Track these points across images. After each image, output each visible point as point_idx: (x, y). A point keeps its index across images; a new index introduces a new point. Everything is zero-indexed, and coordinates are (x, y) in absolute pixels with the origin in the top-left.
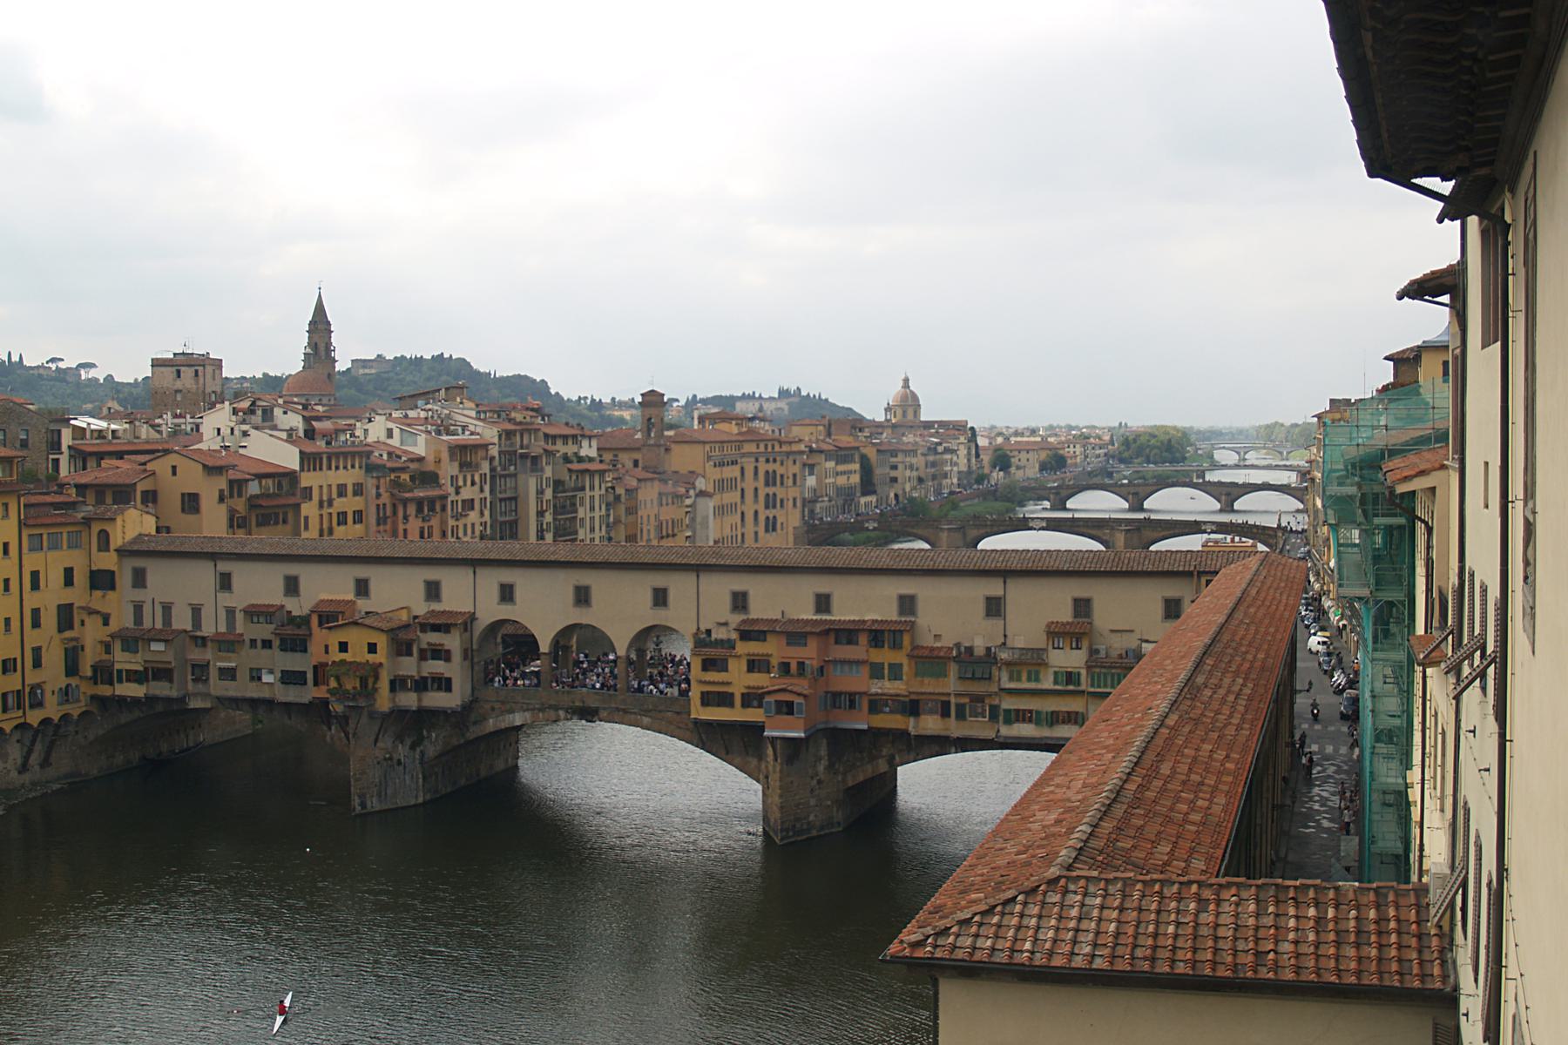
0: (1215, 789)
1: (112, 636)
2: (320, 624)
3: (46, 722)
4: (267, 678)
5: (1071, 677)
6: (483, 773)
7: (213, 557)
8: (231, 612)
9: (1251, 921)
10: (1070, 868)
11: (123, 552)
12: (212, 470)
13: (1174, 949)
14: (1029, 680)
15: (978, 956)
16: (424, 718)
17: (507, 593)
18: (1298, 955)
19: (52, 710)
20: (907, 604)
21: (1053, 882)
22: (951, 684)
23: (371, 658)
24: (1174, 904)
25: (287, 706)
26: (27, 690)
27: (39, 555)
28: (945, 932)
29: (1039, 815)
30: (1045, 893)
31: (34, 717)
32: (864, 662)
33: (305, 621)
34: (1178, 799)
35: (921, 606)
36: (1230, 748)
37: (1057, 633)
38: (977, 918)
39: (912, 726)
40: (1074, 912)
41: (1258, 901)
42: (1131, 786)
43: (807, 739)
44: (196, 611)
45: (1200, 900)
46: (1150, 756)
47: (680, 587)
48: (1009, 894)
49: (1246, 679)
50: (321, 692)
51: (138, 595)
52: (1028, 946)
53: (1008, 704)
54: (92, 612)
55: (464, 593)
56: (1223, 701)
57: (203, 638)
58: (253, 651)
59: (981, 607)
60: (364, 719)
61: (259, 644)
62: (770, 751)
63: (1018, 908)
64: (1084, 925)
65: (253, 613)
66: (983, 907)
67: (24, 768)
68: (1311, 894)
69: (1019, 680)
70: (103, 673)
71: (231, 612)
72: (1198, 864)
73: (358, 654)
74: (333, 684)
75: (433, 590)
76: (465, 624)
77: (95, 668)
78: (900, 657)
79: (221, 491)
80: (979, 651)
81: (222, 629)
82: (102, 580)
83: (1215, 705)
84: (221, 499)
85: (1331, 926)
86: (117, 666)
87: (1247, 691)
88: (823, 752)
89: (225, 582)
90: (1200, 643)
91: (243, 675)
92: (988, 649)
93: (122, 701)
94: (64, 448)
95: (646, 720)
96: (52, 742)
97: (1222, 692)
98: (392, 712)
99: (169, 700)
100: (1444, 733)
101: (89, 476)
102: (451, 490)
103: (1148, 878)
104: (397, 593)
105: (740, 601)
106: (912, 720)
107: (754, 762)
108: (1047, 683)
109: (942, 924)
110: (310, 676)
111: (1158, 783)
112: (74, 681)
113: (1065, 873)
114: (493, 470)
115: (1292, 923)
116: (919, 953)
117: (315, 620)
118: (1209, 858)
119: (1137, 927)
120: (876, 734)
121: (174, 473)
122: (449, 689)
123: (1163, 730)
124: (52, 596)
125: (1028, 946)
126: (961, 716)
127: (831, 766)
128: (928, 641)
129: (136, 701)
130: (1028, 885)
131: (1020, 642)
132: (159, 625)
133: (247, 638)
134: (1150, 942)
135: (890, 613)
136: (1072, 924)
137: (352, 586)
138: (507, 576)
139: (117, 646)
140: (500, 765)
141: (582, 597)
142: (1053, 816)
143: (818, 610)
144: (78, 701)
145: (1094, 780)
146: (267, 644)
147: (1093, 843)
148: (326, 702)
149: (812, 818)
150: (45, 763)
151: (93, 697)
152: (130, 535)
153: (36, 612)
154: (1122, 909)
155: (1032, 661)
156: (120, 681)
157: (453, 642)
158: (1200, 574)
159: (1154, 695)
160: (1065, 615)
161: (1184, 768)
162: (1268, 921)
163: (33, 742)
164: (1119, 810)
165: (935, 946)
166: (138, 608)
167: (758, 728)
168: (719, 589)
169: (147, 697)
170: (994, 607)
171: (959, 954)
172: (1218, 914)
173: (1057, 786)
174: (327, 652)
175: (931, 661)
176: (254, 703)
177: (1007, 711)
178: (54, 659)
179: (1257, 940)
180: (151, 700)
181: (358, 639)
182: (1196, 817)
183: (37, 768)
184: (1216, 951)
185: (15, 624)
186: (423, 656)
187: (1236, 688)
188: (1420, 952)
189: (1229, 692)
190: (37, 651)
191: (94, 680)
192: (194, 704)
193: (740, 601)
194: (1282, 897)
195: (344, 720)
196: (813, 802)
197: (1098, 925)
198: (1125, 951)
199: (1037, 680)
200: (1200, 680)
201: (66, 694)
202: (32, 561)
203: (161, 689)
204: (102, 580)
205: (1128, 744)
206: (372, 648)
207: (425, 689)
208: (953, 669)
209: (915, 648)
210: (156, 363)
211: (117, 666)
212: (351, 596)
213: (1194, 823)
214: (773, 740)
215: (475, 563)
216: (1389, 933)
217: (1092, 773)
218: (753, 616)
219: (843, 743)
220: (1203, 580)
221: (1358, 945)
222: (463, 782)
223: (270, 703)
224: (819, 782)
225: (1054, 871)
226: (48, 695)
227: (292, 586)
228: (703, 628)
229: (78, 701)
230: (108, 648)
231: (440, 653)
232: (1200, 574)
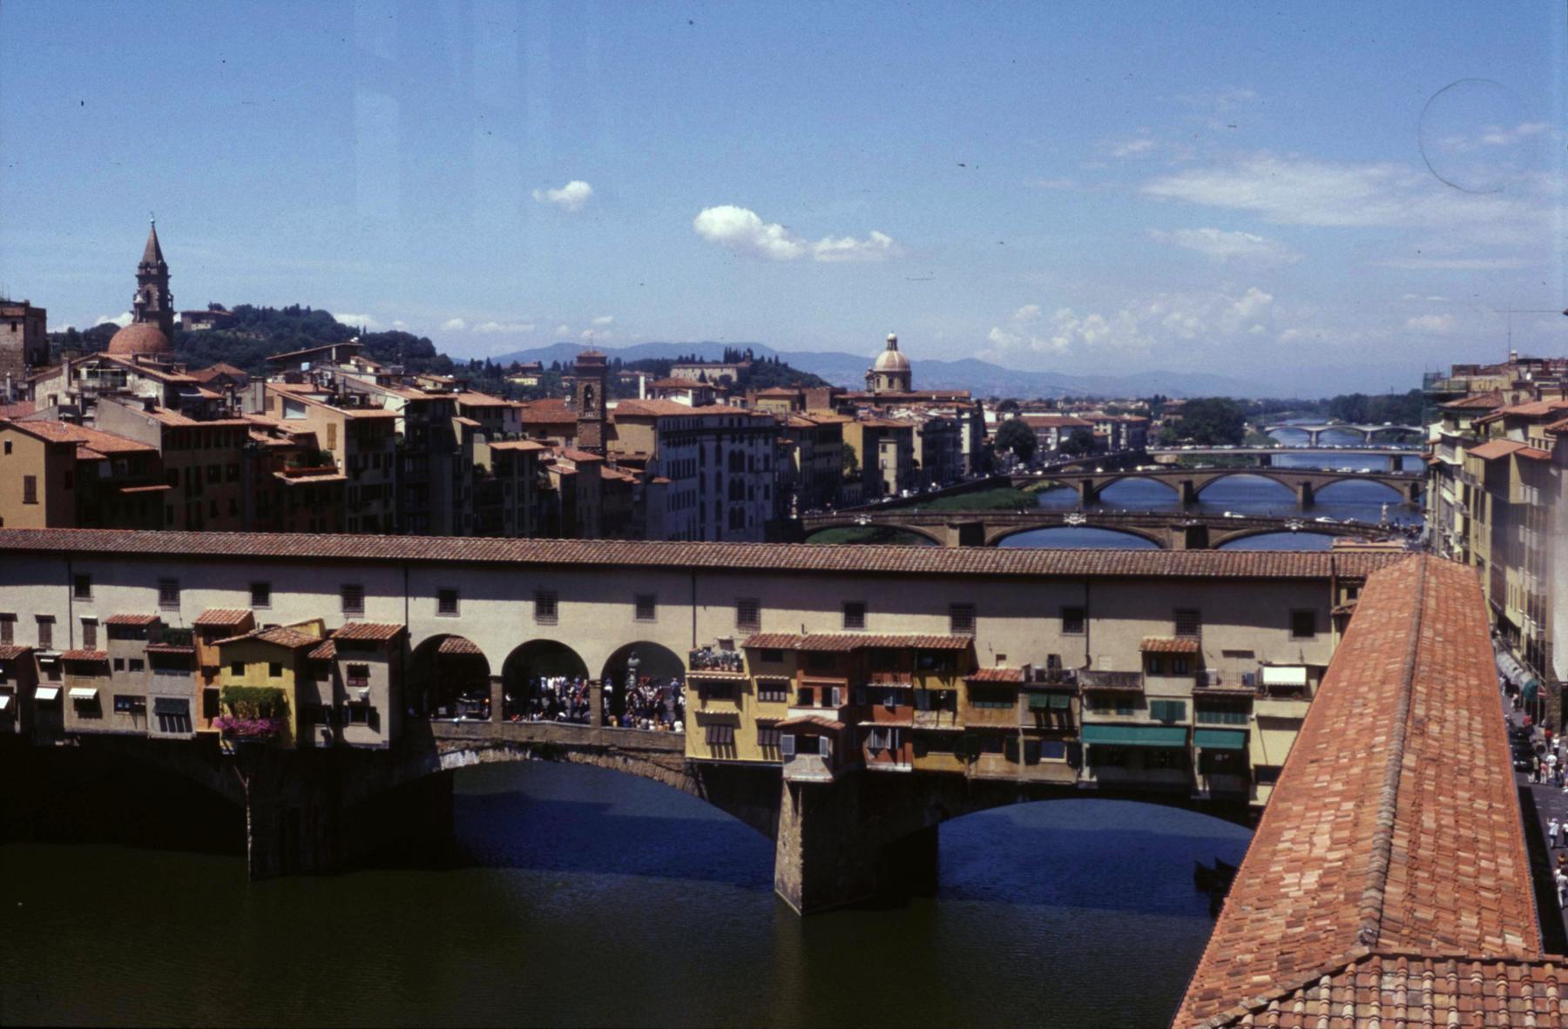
22: (1019, 717)
24: (1525, 990)
29: (1290, 878)
30: (1355, 975)
36: (1487, 793)
38: (1274, 1005)
40: (1399, 998)
44: (45, 622)
46: (1404, 803)
49: (1469, 709)
58: (117, 674)
62: (787, 799)
64: (1414, 1014)
66: (1279, 992)
71: (90, 624)
73: (257, 676)
76: (394, 637)
87: (1477, 724)
97: (1449, 728)
110: (196, 709)
118: (1525, 933)
119: (1484, 1017)
122: (374, 724)
136: (1400, 1013)
142: (1311, 879)
145: (1345, 834)
146: (136, 665)
147: (1388, 912)
148: (213, 737)
158: (1340, 582)
159: (1372, 729)
161: (1447, 821)
164: (1398, 872)
173: (1293, 841)
187: (1465, 722)
189: (1458, 727)
197: (1432, 1014)
200: (1420, 711)
213: (1488, 889)
214: (795, 786)
217: (1336, 827)
220: (1344, 593)
223: (140, 740)
228: (699, 646)
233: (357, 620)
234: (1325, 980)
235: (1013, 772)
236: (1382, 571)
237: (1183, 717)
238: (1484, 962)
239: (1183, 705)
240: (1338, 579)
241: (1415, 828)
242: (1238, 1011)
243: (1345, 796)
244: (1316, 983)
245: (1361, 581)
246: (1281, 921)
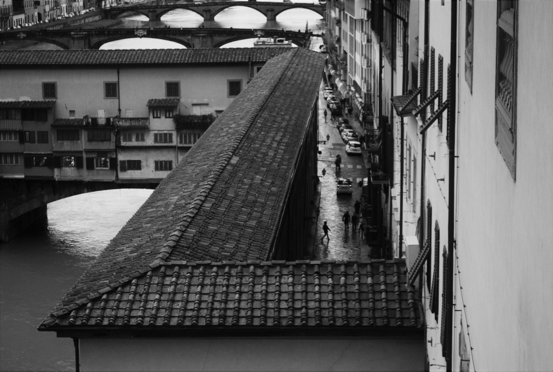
0: (264, 205)
5: (167, 137)
10: (167, 259)
13: (238, 310)
14: (137, 140)
18: (321, 309)
21: (156, 270)
30: (151, 277)
34: (240, 212)
35: (60, 91)
37: (156, 107)
39: (57, 174)
42: (208, 205)
48: (126, 279)
53: (122, 157)
56: (269, 147)
59: (101, 91)
63: (133, 288)
69: (130, 140)
78: (45, 127)
80: (102, 122)
92: (108, 120)
100: (415, 161)
106: (56, 171)
108: (150, 141)
111: (226, 202)
116: (66, 323)
123: (229, 167)
126: (90, 167)
128: (64, 115)
131: (130, 115)
135: (37, 96)
155: (139, 128)
160: (161, 94)
161: (242, 192)
162: (299, 288)
165: (76, 318)
170: (112, 90)
172: (267, 285)
177: (123, 162)
187: (278, 138)
188: (400, 304)
199: (143, 140)
205: (205, 177)
208: (84, 135)
209: (57, 120)
216: (381, 292)
217: (183, 197)
220: (255, 68)
221: (360, 301)
225: (156, 262)
232: (254, 64)
235: (81, 176)
236: (275, 57)
237: (171, 141)
238: (218, 266)
239: (171, 135)
240: (252, 62)
242: (84, 300)
243: (193, 182)
244: (129, 283)
245: (263, 63)
246: (129, 250)
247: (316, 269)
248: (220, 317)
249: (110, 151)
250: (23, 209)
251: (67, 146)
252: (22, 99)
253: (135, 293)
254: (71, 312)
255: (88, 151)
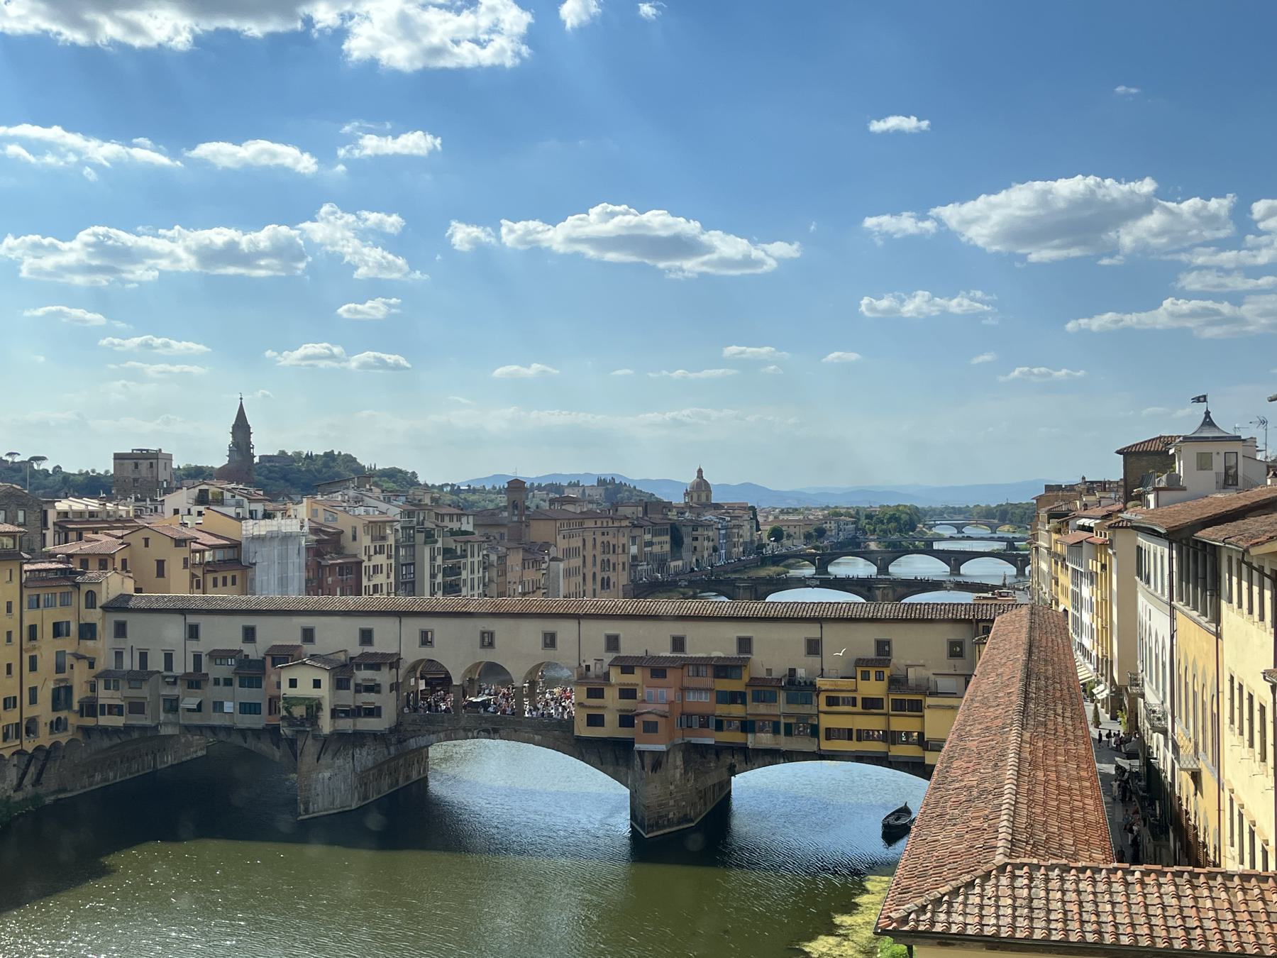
1: (97, 677)
2: (274, 665)
3: (38, 749)
4: (228, 707)
6: (402, 783)
7: (183, 612)
8: (197, 658)
9: (1174, 902)
11: (106, 608)
12: (180, 543)
15: (954, 929)
16: (358, 738)
17: (426, 640)
18: (1221, 932)
19: (45, 738)
20: (745, 644)
21: (1002, 869)
23: (315, 693)
25: (243, 732)
26: (24, 723)
27: (38, 612)
28: (923, 909)
30: (997, 877)
31: (29, 746)
32: (711, 690)
33: (260, 665)
35: (755, 647)
38: (946, 898)
39: (752, 741)
40: (1025, 892)
41: (1176, 885)
43: (668, 752)
44: (169, 658)
45: (1127, 884)
47: (565, 631)
48: (967, 878)
50: (274, 720)
51: (121, 643)
52: (993, 921)
53: (826, 722)
54: (79, 657)
55: (387, 637)
57: (176, 678)
59: (802, 648)
60: (310, 741)
61: (222, 681)
62: (637, 761)
63: (977, 890)
65: (218, 656)
66: (947, 888)
67: (19, 787)
68: (1219, 879)
70: (90, 708)
72: (1098, 856)
73: (305, 689)
74: (284, 713)
75: (366, 637)
77: (81, 703)
79: (186, 560)
81: (190, 669)
82: (88, 631)
83: (1051, 725)
84: (185, 567)
85: (1243, 907)
86: (101, 702)
88: (679, 762)
89: (193, 632)
90: (1019, 675)
91: (208, 707)
93: (106, 731)
94: (50, 524)
95: (537, 738)
96: (43, 766)
98: (332, 734)
99: (144, 728)
101: (72, 548)
102: (365, 558)
103: (1079, 865)
104: (338, 637)
105: (613, 643)
106: (750, 736)
107: (623, 769)
109: (920, 901)
110: (265, 708)
112: (63, 714)
113: (1007, 860)
114: (396, 541)
115: (1209, 904)
117: (269, 660)
120: (719, 750)
121: (147, 545)
122: (379, 715)
124: (47, 649)
125: (993, 921)
126: (789, 732)
127: (686, 772)
129: (116, 731)
130: (979, 872)
132: (136, 667)
133: (211, 677)
134: (1094, 918)
135: (732, 651)
137: (299, 634)
138: (426, 624)
139: (101, 684)
140: (415, 776)
141: (488, 641)
143: (675, 649)
144: (65, 729)
146: (228, 682)
148: (276, 729)
149: (671, 815)
150: (37, 782)
151: (80, 728)
152: (112, 596)
153: (33, 660)
154: (1064, 892)
156: (103, 713)
157: (384, 677)
158: (978, 621)
160: (871, 653)
163: (28, 766)
165: (917, 921)
166: (119, 655)
167: (627, 744)
168: (597, 632)
169: (126, 726)
170: (814, 647)
171: (939, 928)
174: (279, 685)
175: (764, 689)
176: (213, 729)
177: (828, 730)
178: (45, 696)
179: (1183, 918)
180: (128, 729)
181: (305, 677)
182: (1077, 815)
183: (30, 788)
184: (1151, 927)
185: (16, 670)
186: (359, 689)
190: (33, 691)
191: (81, 713)
192: (164, 731)
193: (613, 643)
194: (1229, 884)
195: (292, 743)
196: (672, 803)
198: (1074, 925)
201: (57, 725)
202: (30, 617)
203: (137, 720)
204: (88, 631)
205: (1003, 755)
206: (317, 684)
207: (359, 715)
208: (782, 696)
210: (118, 457)
211: (101, 702)
212: (299, 643)
214: (641, 753)
215: (400, 614)
218: (623, 654)
219: (695, 753)
222: (386, 790)
223: (229, 730)
224: (676, 786)
225: (999, 859)
226: (41, 725)
227: (249, 634)
229: (65, 729)
230: (93, 688)
231: (373, 688)
233: (368, 649)
234: (977, 881)
241: (1033, 782)
244: (971, 885)
245: (992, 621)
247: (1202, 879)
248: (1095, 932)
249: (811, 716)
250: (712, 779)
251: (762, 709)
252: (715, 654)
253: (982, 896)
254: (910, 914)
255: (787, 715)
